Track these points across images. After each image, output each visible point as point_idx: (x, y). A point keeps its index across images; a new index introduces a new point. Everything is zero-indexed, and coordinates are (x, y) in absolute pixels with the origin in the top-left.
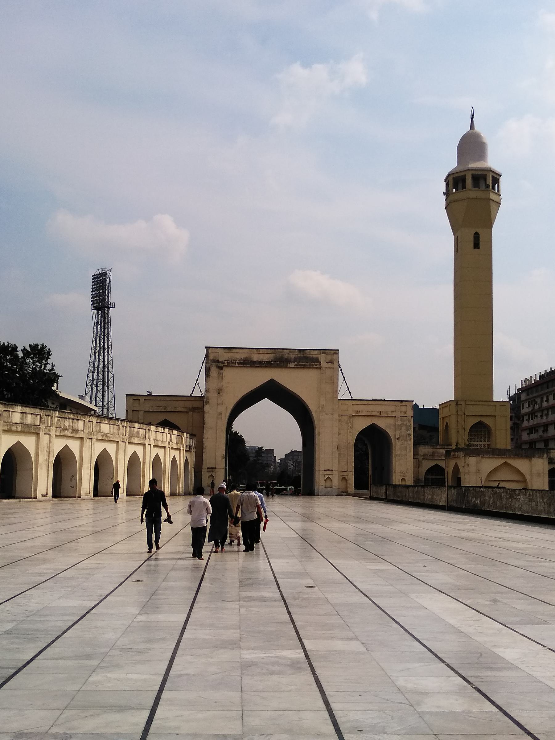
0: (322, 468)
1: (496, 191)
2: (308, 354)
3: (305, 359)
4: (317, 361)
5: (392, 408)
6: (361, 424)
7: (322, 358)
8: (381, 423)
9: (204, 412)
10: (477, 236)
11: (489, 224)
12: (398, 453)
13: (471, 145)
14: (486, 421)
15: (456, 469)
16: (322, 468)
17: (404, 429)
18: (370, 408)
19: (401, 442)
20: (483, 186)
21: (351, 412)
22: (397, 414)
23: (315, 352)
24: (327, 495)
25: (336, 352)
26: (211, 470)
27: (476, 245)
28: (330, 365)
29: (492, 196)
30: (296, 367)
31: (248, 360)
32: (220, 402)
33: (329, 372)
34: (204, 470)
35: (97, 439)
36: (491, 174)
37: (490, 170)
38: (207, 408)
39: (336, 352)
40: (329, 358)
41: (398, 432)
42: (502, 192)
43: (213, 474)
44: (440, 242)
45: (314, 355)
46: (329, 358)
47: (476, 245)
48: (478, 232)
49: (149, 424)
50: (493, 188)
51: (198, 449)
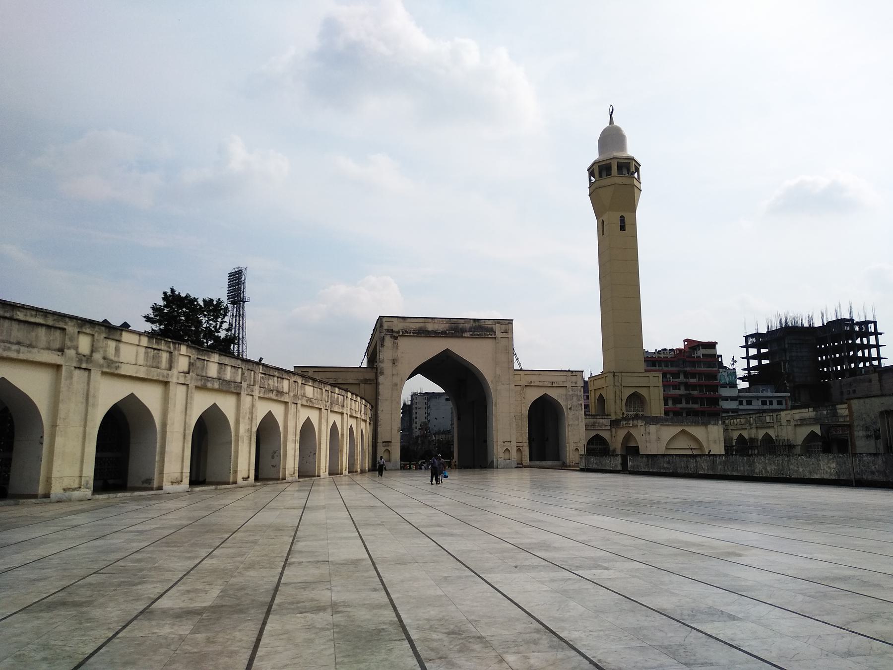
0: (500, 440)
2: (482, 324)
3: (480, 329)
4: (491, 330)
5: (563, 378)
6: (534, 395)
7: (497, 328)
8: (553, 394)
9: (377, 384)
12: (571, 423)
14: (640, 391)
15: (629, 437)
16: (500, 440)
17: (575, 398)
18: (542, 378)
19: (573, 412)
21: (523, 383)
22: (569, 384)
23: (490, 322)
24: (506, 467)
25: (510, 322)
26: (387, 443)
28: (504, 335)
30: (472, 337)
31: (422, 329)
32: (394, 372)
33: (504, 342)
34: (379, 445)
35: (302, 405)
38: (381, 379)
39: (510, 322)
40: (503, 327)
41: (569, 403)
43: (389, 448)
45: (489, 325)
46: (503, 327)
49: (347, 390)
51: (375, 422)
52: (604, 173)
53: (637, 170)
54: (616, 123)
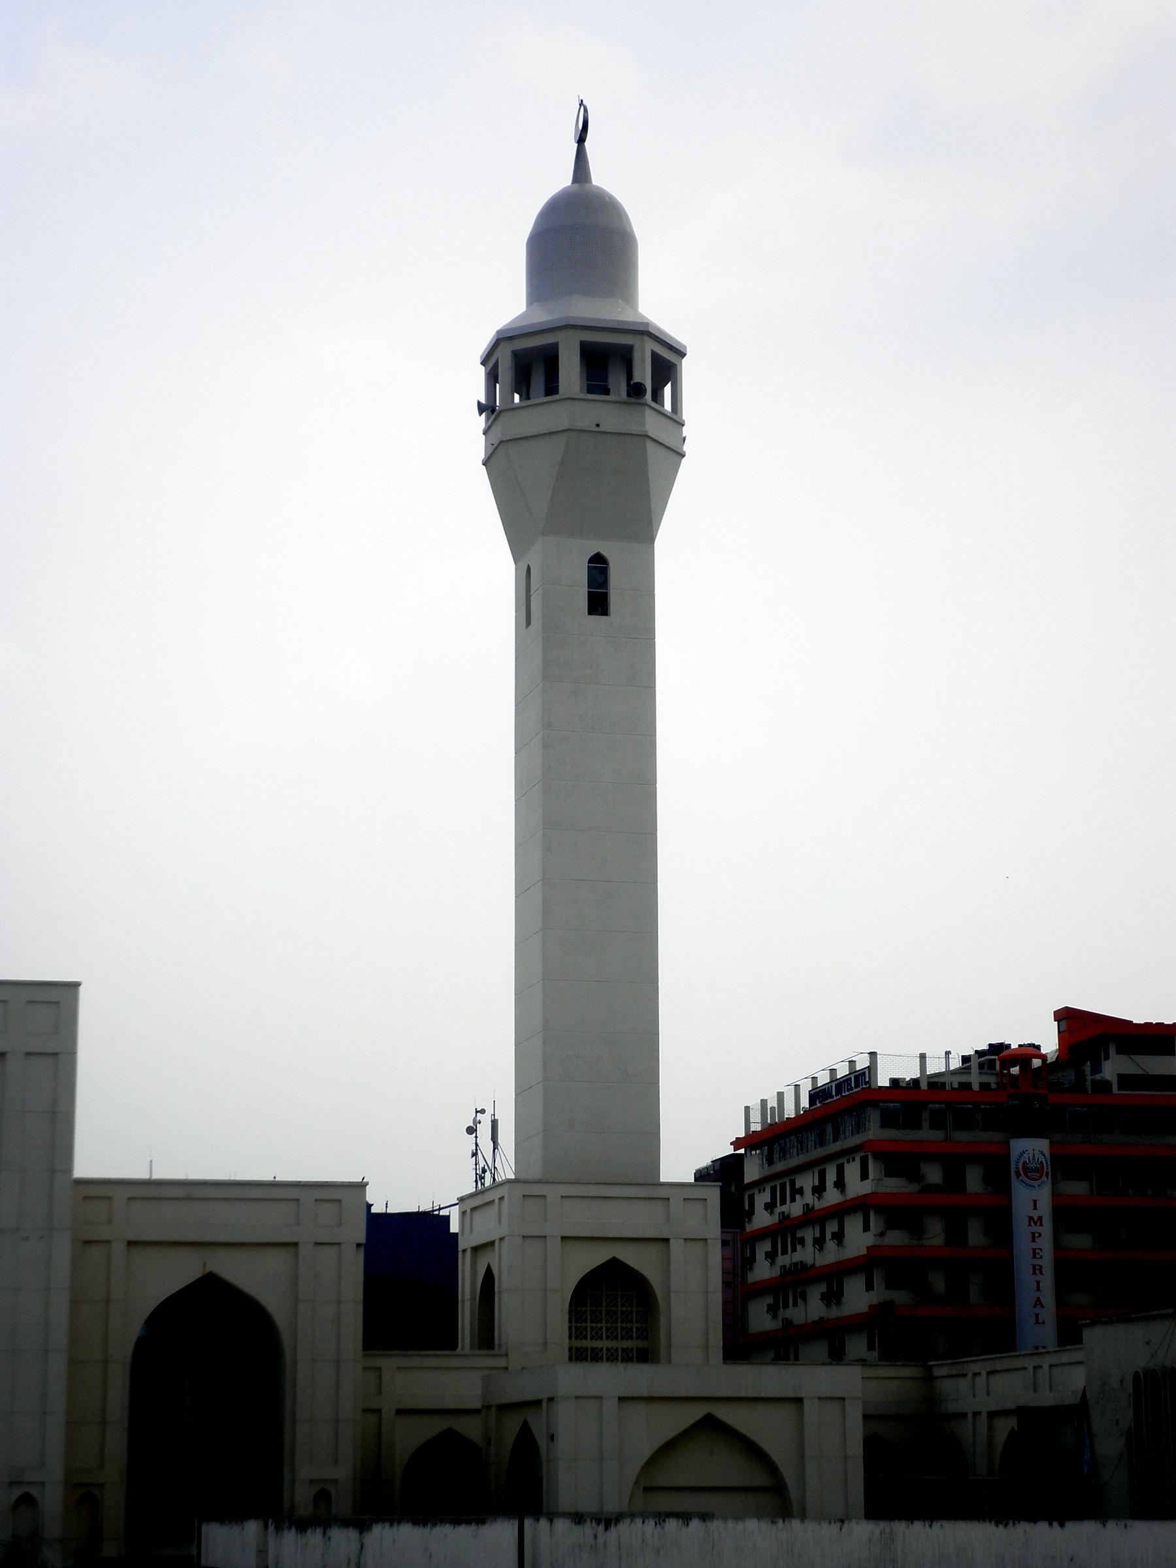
1: (668, 406)
10: (598, 567)
11: (641, 526)
13: (580, 236)
20: (618, 386)
27: (598, 603)
29: (652, 425)
36: (650, 346)
37: (645, 332)
42: (687, 414)
44: (462, 572)
47: (598, 603)
48: (604, 553)
50: (657, 396)
52: (538, 382)
53: (666, 369)
54: (600, 178)
